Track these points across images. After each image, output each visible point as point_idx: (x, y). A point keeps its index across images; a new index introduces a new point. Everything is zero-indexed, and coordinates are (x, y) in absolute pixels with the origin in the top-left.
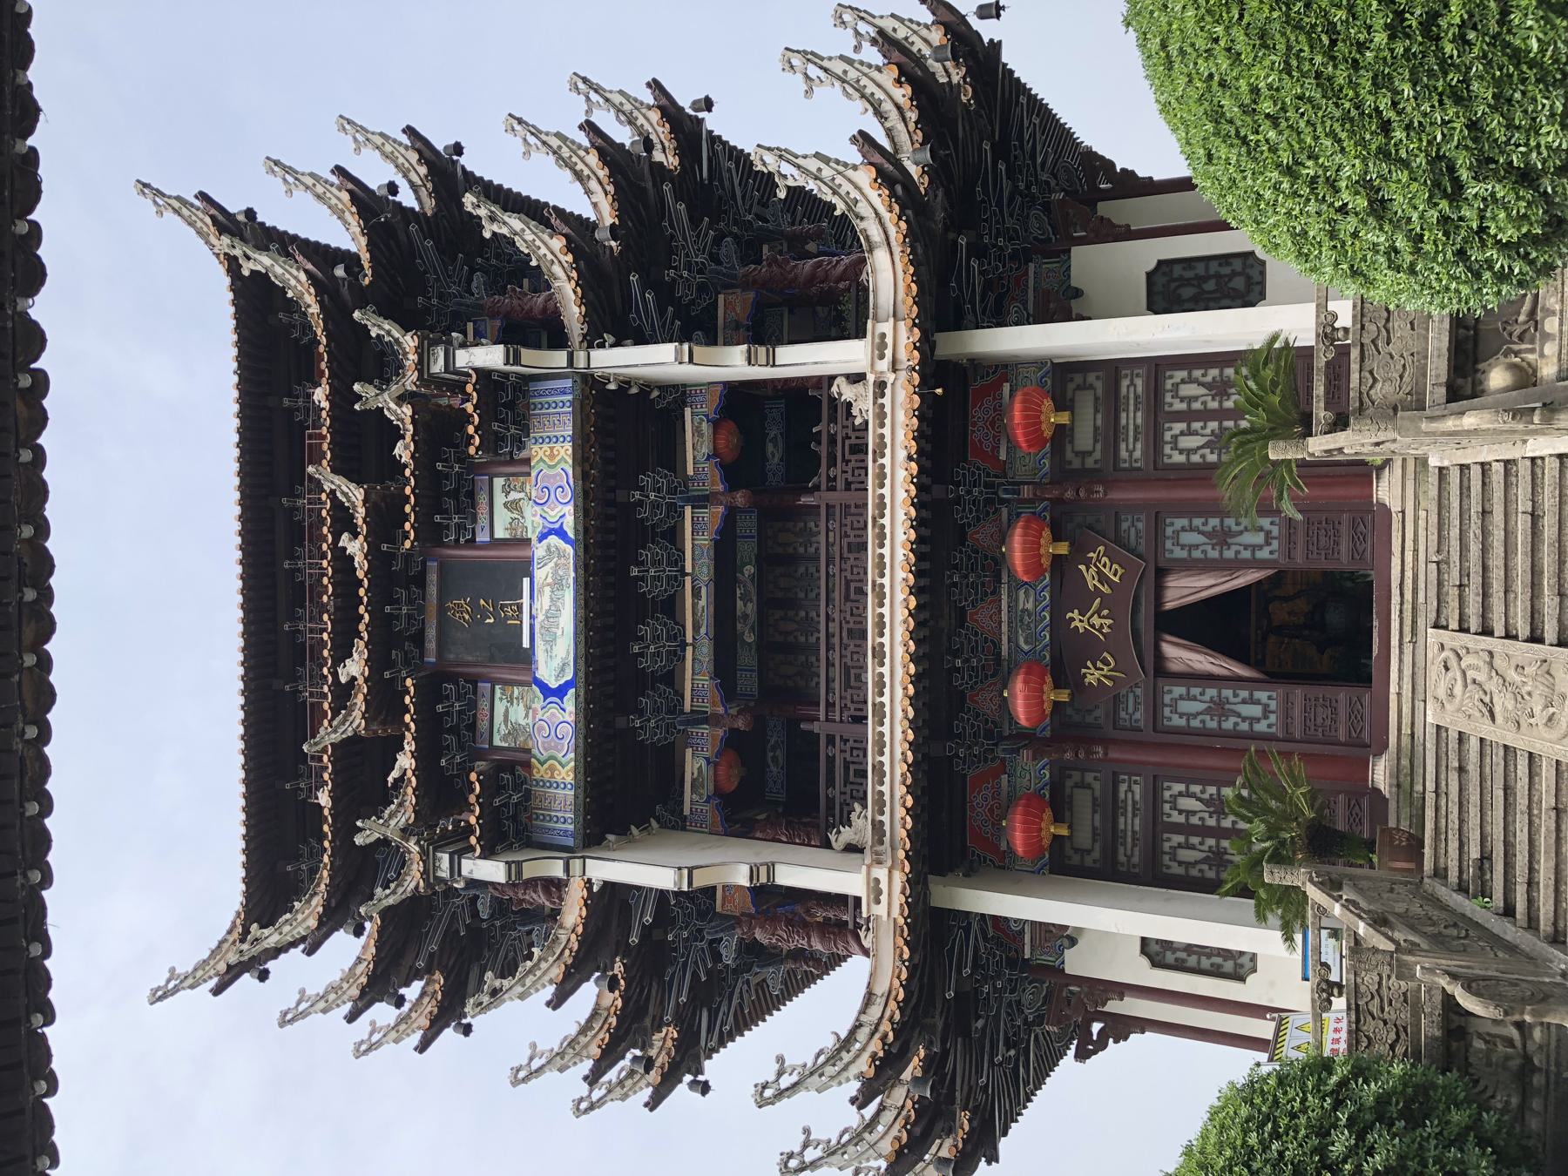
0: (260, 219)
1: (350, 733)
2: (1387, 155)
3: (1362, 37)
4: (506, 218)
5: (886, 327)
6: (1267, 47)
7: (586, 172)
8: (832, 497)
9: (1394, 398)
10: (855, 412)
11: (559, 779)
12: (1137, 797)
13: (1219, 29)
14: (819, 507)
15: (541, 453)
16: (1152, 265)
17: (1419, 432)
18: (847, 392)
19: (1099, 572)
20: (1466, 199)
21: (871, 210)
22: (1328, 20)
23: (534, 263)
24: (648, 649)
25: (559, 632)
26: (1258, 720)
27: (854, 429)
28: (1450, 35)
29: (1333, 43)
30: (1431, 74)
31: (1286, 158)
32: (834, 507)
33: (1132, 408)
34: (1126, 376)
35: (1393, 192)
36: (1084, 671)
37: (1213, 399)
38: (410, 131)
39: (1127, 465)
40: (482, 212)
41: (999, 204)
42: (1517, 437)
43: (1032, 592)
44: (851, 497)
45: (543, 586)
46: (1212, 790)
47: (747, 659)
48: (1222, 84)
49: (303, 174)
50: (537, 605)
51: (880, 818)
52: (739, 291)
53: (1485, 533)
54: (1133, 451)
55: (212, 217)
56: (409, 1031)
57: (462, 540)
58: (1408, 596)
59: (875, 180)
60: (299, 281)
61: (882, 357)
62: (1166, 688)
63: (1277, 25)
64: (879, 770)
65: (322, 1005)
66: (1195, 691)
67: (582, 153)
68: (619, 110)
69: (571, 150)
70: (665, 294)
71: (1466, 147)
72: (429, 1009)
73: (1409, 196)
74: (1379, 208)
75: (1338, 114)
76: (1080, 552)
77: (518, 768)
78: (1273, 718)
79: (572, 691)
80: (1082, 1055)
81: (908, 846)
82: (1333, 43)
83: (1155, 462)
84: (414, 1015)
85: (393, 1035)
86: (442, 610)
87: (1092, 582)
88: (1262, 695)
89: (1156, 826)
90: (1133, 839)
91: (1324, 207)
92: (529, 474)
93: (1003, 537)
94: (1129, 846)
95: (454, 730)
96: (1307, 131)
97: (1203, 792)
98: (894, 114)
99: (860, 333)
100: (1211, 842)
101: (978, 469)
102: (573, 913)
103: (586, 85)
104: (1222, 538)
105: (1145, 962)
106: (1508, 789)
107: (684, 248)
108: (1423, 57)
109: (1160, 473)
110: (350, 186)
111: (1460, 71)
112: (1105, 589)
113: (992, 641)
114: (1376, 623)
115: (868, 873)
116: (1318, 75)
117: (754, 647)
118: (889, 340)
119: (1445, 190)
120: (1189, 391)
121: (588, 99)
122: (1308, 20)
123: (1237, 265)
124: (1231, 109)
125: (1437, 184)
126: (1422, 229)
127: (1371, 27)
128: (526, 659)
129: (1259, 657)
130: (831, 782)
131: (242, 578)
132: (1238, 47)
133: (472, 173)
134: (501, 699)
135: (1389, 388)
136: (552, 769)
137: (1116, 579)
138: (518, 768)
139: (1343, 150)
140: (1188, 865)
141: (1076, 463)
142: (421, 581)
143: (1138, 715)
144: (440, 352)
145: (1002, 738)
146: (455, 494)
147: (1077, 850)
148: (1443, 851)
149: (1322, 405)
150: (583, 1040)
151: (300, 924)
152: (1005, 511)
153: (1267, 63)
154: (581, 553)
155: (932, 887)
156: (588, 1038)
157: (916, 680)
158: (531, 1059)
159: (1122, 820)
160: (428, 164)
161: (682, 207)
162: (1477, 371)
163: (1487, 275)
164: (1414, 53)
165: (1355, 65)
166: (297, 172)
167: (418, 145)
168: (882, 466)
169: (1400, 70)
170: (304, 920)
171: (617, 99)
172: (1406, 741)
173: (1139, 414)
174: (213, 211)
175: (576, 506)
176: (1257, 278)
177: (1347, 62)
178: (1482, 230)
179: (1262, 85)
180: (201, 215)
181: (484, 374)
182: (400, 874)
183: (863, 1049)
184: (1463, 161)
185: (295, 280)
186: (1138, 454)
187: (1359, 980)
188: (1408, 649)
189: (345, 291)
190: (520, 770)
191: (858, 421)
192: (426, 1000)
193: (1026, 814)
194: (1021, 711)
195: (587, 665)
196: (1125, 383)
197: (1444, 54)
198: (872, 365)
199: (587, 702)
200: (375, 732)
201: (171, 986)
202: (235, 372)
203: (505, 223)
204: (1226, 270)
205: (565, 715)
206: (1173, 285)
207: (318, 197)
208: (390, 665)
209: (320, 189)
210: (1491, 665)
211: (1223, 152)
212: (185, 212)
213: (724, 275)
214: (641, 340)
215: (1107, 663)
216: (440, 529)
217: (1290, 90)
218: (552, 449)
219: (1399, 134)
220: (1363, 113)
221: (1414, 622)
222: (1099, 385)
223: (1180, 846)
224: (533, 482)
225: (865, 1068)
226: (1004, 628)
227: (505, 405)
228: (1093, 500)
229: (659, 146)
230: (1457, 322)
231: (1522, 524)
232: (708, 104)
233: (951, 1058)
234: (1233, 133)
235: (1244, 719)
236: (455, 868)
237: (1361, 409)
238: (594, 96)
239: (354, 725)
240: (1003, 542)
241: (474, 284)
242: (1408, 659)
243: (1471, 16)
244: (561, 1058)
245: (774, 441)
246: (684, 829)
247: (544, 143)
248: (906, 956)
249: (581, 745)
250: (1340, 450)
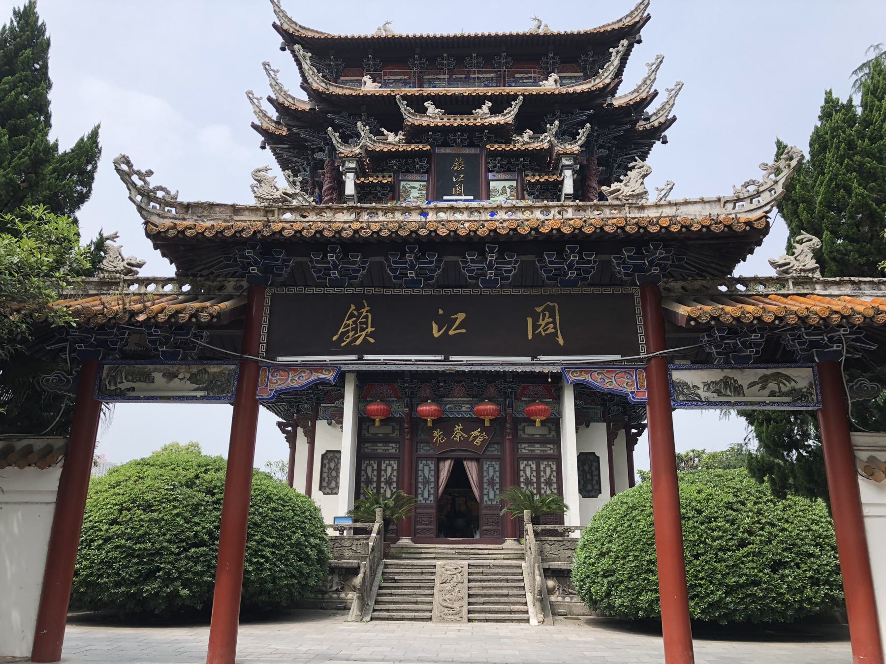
9: (545, 551)
17: (534, 563)
19: (478, 437)
29: (648, 545)
30: (637, 571)
31: (619, 529)
38: (674, 119)
42: (532, 590)
46: (395, 479)
48: (642, 510)
53: (501, 581)
54: (525, 449)
55: (639, 22)
58: (472, 551)
65: (274, 83)
66: (432, 473)
72: (271, 127)
73: (605, 563)
74: (602, 555)
76: (484, 429)
78: (424, 502)
80: (280, 425)
82: (648, 545)
85: (258, 110)
86: (458, 156)
87: (473, 434)
88: (432, 498)
89: (380, 458)
92: (518, 199)
93: (491, 400)
100: (375, 479)
104: (491, 483)
105: (324, 452)
106: (419, 588)
116: (640, 540)
120: (548, 471)
123: (596, 487)
124: (635, 513)
125: (608, 571)
140: (366, 471)
141: (520, 427)
143: (422, 451)
147: (368, 427)
151: (313, 79)
160: (659, 127)
163: (582, 583)
167: (668, 123)
174: (641, 22)
176: (591, 494)
178: (594, 583)
181: (561, 183)
184: (614, 578)
186: (524, 451)
196: (551, 446)
204: (594, 482)
206: (589, 462)
210: (459, 583)
212: (642, 7)
217: (638, 531)
219: (622, 561)
222: (551, 436)
223: (373, 467)
230: (569, 571)
231: (505, 592)
235: (423, 491)
236: (350, 170)
237: (541, 541)
239: (408, 119)
240: (490, 400)
241: (602, 150)
242: (449, 551)
250: (527, 534)
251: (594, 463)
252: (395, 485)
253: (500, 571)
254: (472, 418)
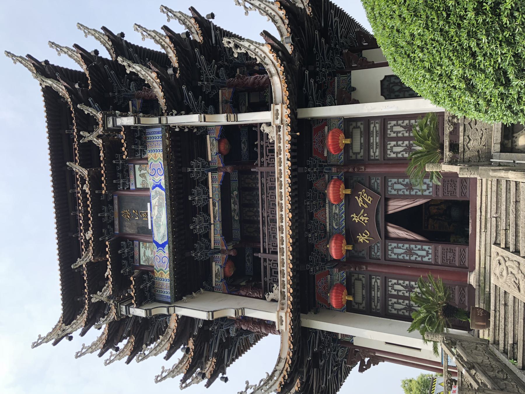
0: (51, 63)
1: (88, 261)
2: (474, 67)
3: (462, 13)
4: (134, 66)
5: (279, 107)
6: (417, 16)
7: (166, 45)
8: (264, 169)
10: (270, 137)
11: (164, 277)
12: (379, 284)
13: (395, 7)
14: (258, 172)
15: (151, 156)
16: (382, 78)
18: (266, 129)
20: (512, 86)
21: (270, 61)
22: (446, 5)
23: (146, 82)
24: (197, 228)
25: (161, 224)
26: (425, 257)
27: (270, 143)
28: (506, 14)
29: (448, 16)
30: (496, 32)
31: (427, 65)
32: (263, 172)
33: (375, 136)
34: (372, 123)
35: (475, 81)
36: (358, 237)
37: (406, 133)
38: (104, 28)
39: (373, 158)
40: (125, 64)
41: (323, 55)
43: (338, 206)
44: (269, 169)
45: (155, 206)
46: (407, 282)
47: (236, 226)
48: (398, 31)
49: (63, 47)
50: (153, 213)
51: (283, 290)
52: (227, 88)
54: (376, 153)
56: (124, 356)
57: (125, 188)
59: (271, 50)
60: (63, 89)
61: (277, 118)
62: (389, 244)
63: (421, 7)
64: (282, 272)
66: (400, 245)
67: (164, 38)
68: (179, 19)
69: (159, 37)
70: (197, 91)
71: (513, 65)
72: (130, 348)
74: (471, 88)
75: (451, 48)
76: (355, 192)
77: (150, 272)
78: (430, 256)
79: (167, 246)
80: (361, 370)
81: (291, 307)
82: (448, 16)
83: (384, 157)
84: (125, 350)
85: (118, 357)
86: (120, 214)
88: (426, 247)
89: (386, 296)
90: (378, 300)
91: (446, 86)
92: (147, 164)
93: (326, 187)
94: (376, 302)
95: (126, 259)
96: (437, 55)
97: (403, 283)
98: (280, 21)
99: (268, 109)
101: (317, 159)
102: (173, 324)
103: (166, 10)
104: (410, 187)
107: (205, 73)
108: (492, 24)
109: (387, 162)
110: (81, 52)
111: (510, 31)
112: (366, 206)
113: (323, 225)
114: (470, 221)
115: (278, 314)
116: (441, 30)
117: (238, 221)
118: (280, 112)
119: (502, 82)
121: (168, 15)
122: (435, 4)
125: (498, 80)
126: (491, 97)
127: (466, 9)
128: (150, 233)
129: (426, 225)
130: (265, 275)
131: (54, 197)
132: (404, 15)
133: (130, 43)
134: (142, 247)
135: (476, 143)
136: (161, 274)
137: (370, 202)
138: (150, 272)
139: (453, 64)
140: (398, 310)
141: (354, 157)
142: (112, 202)
143: (378, 254)
144: (111, 119)
145: (327, 262)
146: (122, 171)
148: (497, 334)
149: (448, 150)
150: (181, 366)
151: (78, 325)
152: (327, 176)
153: (417, 24)
154: (168, 194)
155: (302, 319)
156: (182, 365)
157: (293, 245)
158: (162, 373)
159: (373, 292)
161: (203, 57)
162: (513, 137)
164: (488, 22)
165: (459, 26)
166: (61, 47)
167: (108, 34)
168: (280, 158)
169: (481, 30)
170: (80, 323)
171: (179, 15)
172: (482, 270)
173: (378, 138)
174: (33, 62)
175: (165, 176)
177: (455, 24)
179: (415, 33)
180: (29, 63)
181: (127, 128)
182: (108, 313)
183: (277, 380)
185: (61, 88)
186: (377, 154)
187: (463, 380)
188: (483, 234)
189: (80, 93)
190: (150, 274)
191: (271, 141)
192: (130, 344)
193: (336, 293)
194: (334, 254)
195: (173, 235)
196: (372, 126)
197: (502, 22)
198: (274, 122)
199: (173, 249)
200: (97, 260)
201: (39, 342)
202: (46, 122)
203: (133, 68)
205: (165, 254)
206: (391, 85)
207: (70, 56)
208: (102, 234)
209: (70, 53)
210: (519, 268)
211: (399, 59)
213: (220, 83)
214: (188, 112)
215: (367, 234)
216: (117, 184)
217: (428, 36)
218: (155, 154)
219: (480, 58)
220: (463, 48)
221: (486, 224)
222: (362, 127)
223: (395, 303)
224: (149, 167)
225: (277, 388)
226: (328, 220)
227: (138, 138)
228: (360, 172)
229: (196, 33)
230: (504, 128)
232: (212, 16)
233: (311, 377)
234: (403, 52)
235: (419, 256)
236: (127, 311)
238: (170, 14)
241: (131, 86)
243: (516, 4)
244: (172, 373)
245: (244, 143)
246: (214, 291)
247: (149, 35)
248: (292, 347)
249: (172, 265)
251: (392, 81)
252: (413, 283)
253: (503, 207)
254: (345, 203)
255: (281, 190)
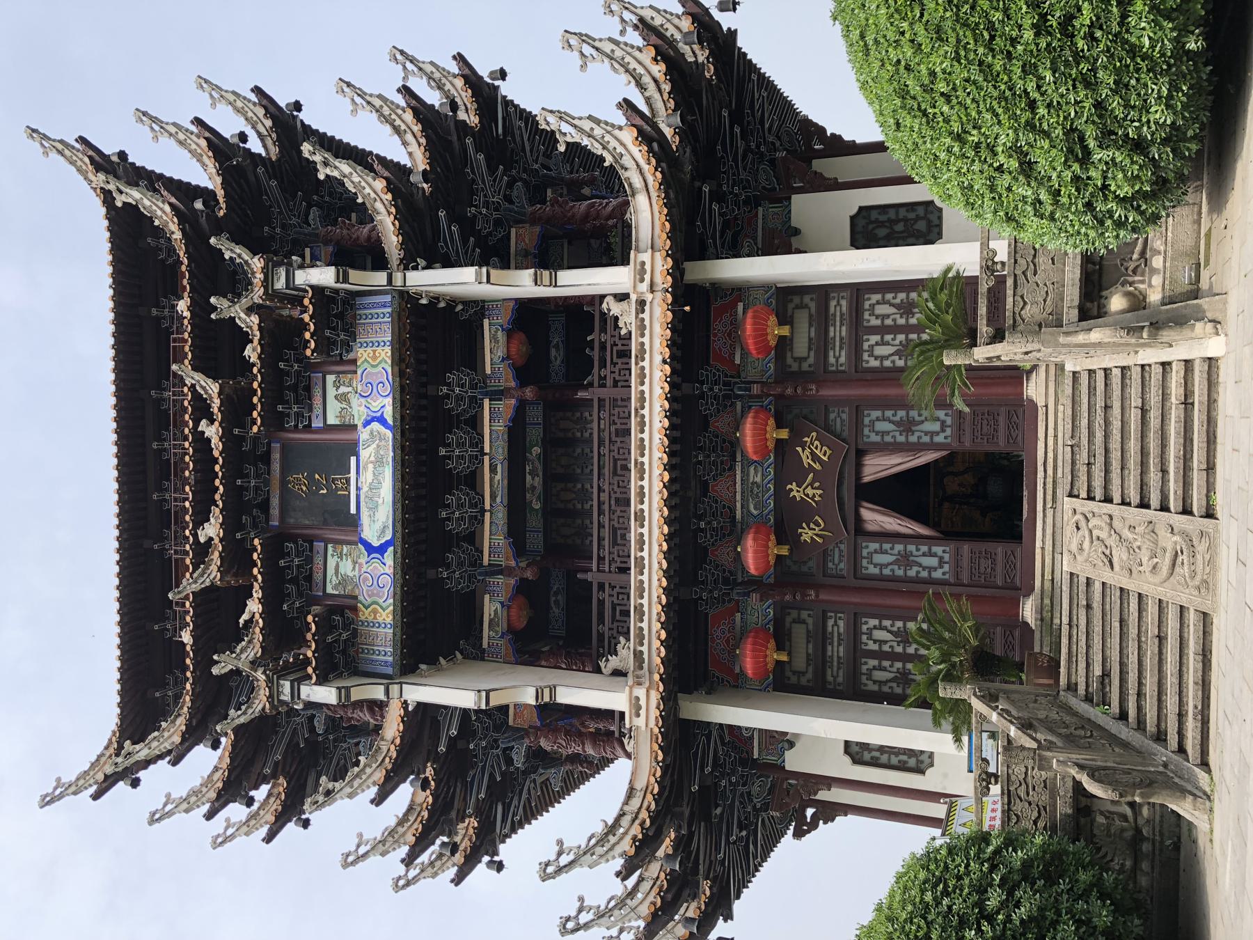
0: (131, 160)
1: (208, 583)
2: (1033, 127)
3: (1014, 34)
4: (337, 164)
5: (646, 257)
6: (942, 40)
7: (403, 127)
8: (605, 393)
9: (1039, 318)
10: (621, 324)
11: (380, 620)
12: (842, 630)
13: (905, 25)
14: (592, 400)
15: (365, 355)
16: (855, 210)
17: (1058, 345)
18: (615, 308)
19: (812, 453)
20: (1093, 163)
21: (633, 162)
22: (988, 19)
23: (360, 200)
24: (454, 515)
25: (380, 501)
26: (935, 569)
27: (620, 338)
28: (1082, 33)
29: (992, 38)
31: (956, 127)
32: (604, 400)
33: (838, 324)
34: (834, 298)
35: (1036, 156)
36: (800, 530)
37: (901, 317)
38: (257, 90)
39: (834, 368)
40: (317, 158)
41: (735, 160)
42: (1131, 349)
43: (760, 469)
44: (618, 393)
45: (367, 464)
46: (899, 624)
47: (535, 522)
48: (908, 68)
49: (167, 124)
50: (362, 479)
51: (640, 648)
52: (527, 225)
53: (1107, 423)
54: (839, 357)
55: (90, 157)
56: (258, 826)
57: (300, 426)
58: (1050, 472)
59: (637, 139)
60: (164, 212)
61: (642, 280)
62: (864, 544)
63: (949, 23)
64: (640, 610)
65: (185, 806)
66: (887, 546)
67: (400, 112)
68: (430, 78)
69: (391, 109)
70: (468, 227)
71: (1094, 122)
72: (274, 807)
73: (1048, 159)
74: (1027, 168)
75: (996, 94)
76: (797, 437)
77: (347, 611)
78: (946, 567)
79: (391, 549)
80: (799, 834)
81: (662, 671)
82: (992, 38)
83: (856, 366)
84: (262, 812)
85: (245, 829)
86: (284, 483)
87: (806, 460)
88: (938, 550)
89: (856, 653)
90: (839, 663)
91: (986, 167)
92: (355, 372)
94: (835, 669)
95: (294, 581)
96: (972, 107)
97: (892, 626)
98: (652, 87)
99: (625, 261)
100: (899, 665)
101: (718, 370)
102: (392, 727)
103: (402, 56)
104: (907, 426)
105: (847, 759)
106: (1122, 622)
107: (483, 190)
108: (1061, 50)
109: (859, 374)
110: (207, 134)
111: (1089, 62)
112: (817, 466)
113: (729, 507)
114: (1025, 493)
115: (631, 693)
116: (981, 63)
117: (540, 511)
118: (648, 267)
119: (1077, 155)
120: (882, 310)
121: (405, 68)
122: (973, 19)
123: (921, 211)
124: (915, 89)
125: (1071, 151)
126: (1059, 185)
127: (1021, 26)
128: (353, 523)
129: (936, 519)
130: (601, 620)
131: (117, 456)
132: (919, 39)
133: (309, 126)
134: (333, 555)
135: (1035, 310)
136: (375, 612)
137: (825, 459)
138: (347, 611)
139: (999, 122)
140: (880, 683)
141: (795, 367)
142: (266, 458)
143: (842, 566)
144: (282, 272)
145: (736, 584)
146: (294, 388)
147: (794, 673)
148: (1074, 670)
149: (985, 322)
150: (400, 830)
151: (166, 740)
152: (739, 405)
153: (941, 52)
154: (399, 437)
155: (679, 702)
156: (405, 828)
157: (669, 538)
158: (358, 846)
159: (829, 648)
160: (273, 117)
161: (481, 157)
162: (1101, 297)
163: (1109, 223)
164: (1054, 48)
165: (1009, 56)
166: (162, 122)
167: (265, 102)
168: (643, 368)
169: (1044, 61)
170: (170, 737)
171: (429, 68)
172: (1048, 585)
173: (844, 328)
174: (91, 153)
175: (394, 399)
176: (936, 222)
177: (1003, 53)
178: (1105, 187)
179: (938, 70)
180: (80, 156)
181: (318, 290)
182: (249, 698)
183: (626, 833)
184: (1090, 133)
185: (161, 211)
186: (843, 360)
187: (1010, 771)
188: (1050, 513)
189: (203, 220)
190: (349, 614)
191: (623, 332)
192: (272, 799)
193: (754, 644)
194: (751, 563)
195: (404, 527)
196: (833, 303)
197: (1077, 48)
198: (635, 287)
199: (404, 558)
200: (229, 582)
201: (58, 792)
202: (111, 287)
203: (336, 167)
204: (912, 215)
205: (384, 570)
206: (871, 227)
207: (180, 143)
208: (241, 527)
209: (181, 136)
210: (1111, 525)
211: (908, 121)
212: (67, 152)
213: (515, 212)
214: (448, 263)
215: (819, 525)
216: (282, 417)
217: (959, 74)
218: (374, 351)
219: (1042, 111)
220: (1015, 94)
221: (1054, 493)
222: (813, 305)
223: (874, 668)
224: (359, 379)
225: (627, 848)
226: (738, 497)
227: (336, 316)
228: (807, 396)
229: (463, 108)
231: (1134, 416)
232: (503, 74)
233: (696, 838)
234: (916, 107)
235: (924, 569)
236: (295, 693)
237: (1014, 326)
238: (409, 66)
239: (212, 577)
240: (737, 429)
241: (311, 217)
242: (1049, 520)
243: (1098, 18)
244: (383, 845)
245: (557, 347)
246: (483, 659)
247: (369, 103)
248: (660, 758)
249: (399, 592)
250: (998, 358)
251: (873, 218)
253: (1084, 422)
255: (642, 436)
